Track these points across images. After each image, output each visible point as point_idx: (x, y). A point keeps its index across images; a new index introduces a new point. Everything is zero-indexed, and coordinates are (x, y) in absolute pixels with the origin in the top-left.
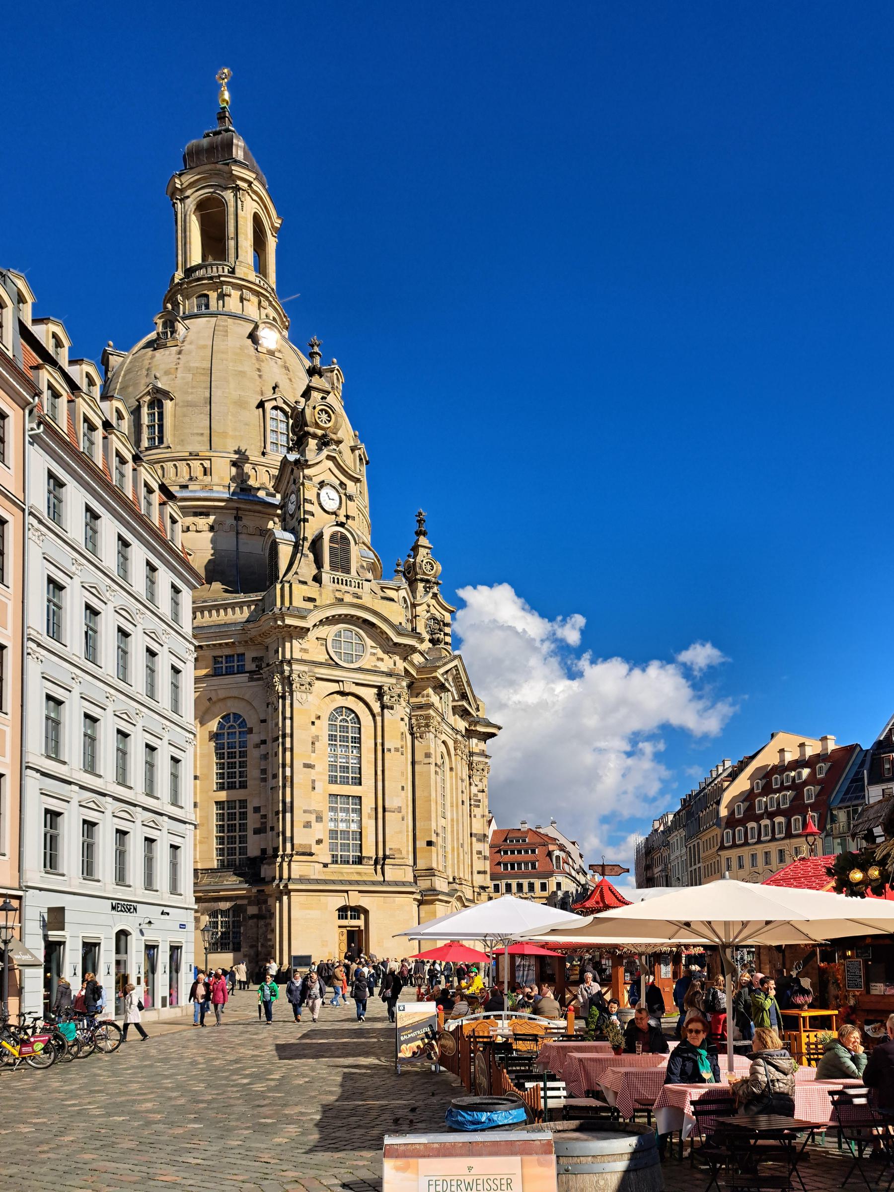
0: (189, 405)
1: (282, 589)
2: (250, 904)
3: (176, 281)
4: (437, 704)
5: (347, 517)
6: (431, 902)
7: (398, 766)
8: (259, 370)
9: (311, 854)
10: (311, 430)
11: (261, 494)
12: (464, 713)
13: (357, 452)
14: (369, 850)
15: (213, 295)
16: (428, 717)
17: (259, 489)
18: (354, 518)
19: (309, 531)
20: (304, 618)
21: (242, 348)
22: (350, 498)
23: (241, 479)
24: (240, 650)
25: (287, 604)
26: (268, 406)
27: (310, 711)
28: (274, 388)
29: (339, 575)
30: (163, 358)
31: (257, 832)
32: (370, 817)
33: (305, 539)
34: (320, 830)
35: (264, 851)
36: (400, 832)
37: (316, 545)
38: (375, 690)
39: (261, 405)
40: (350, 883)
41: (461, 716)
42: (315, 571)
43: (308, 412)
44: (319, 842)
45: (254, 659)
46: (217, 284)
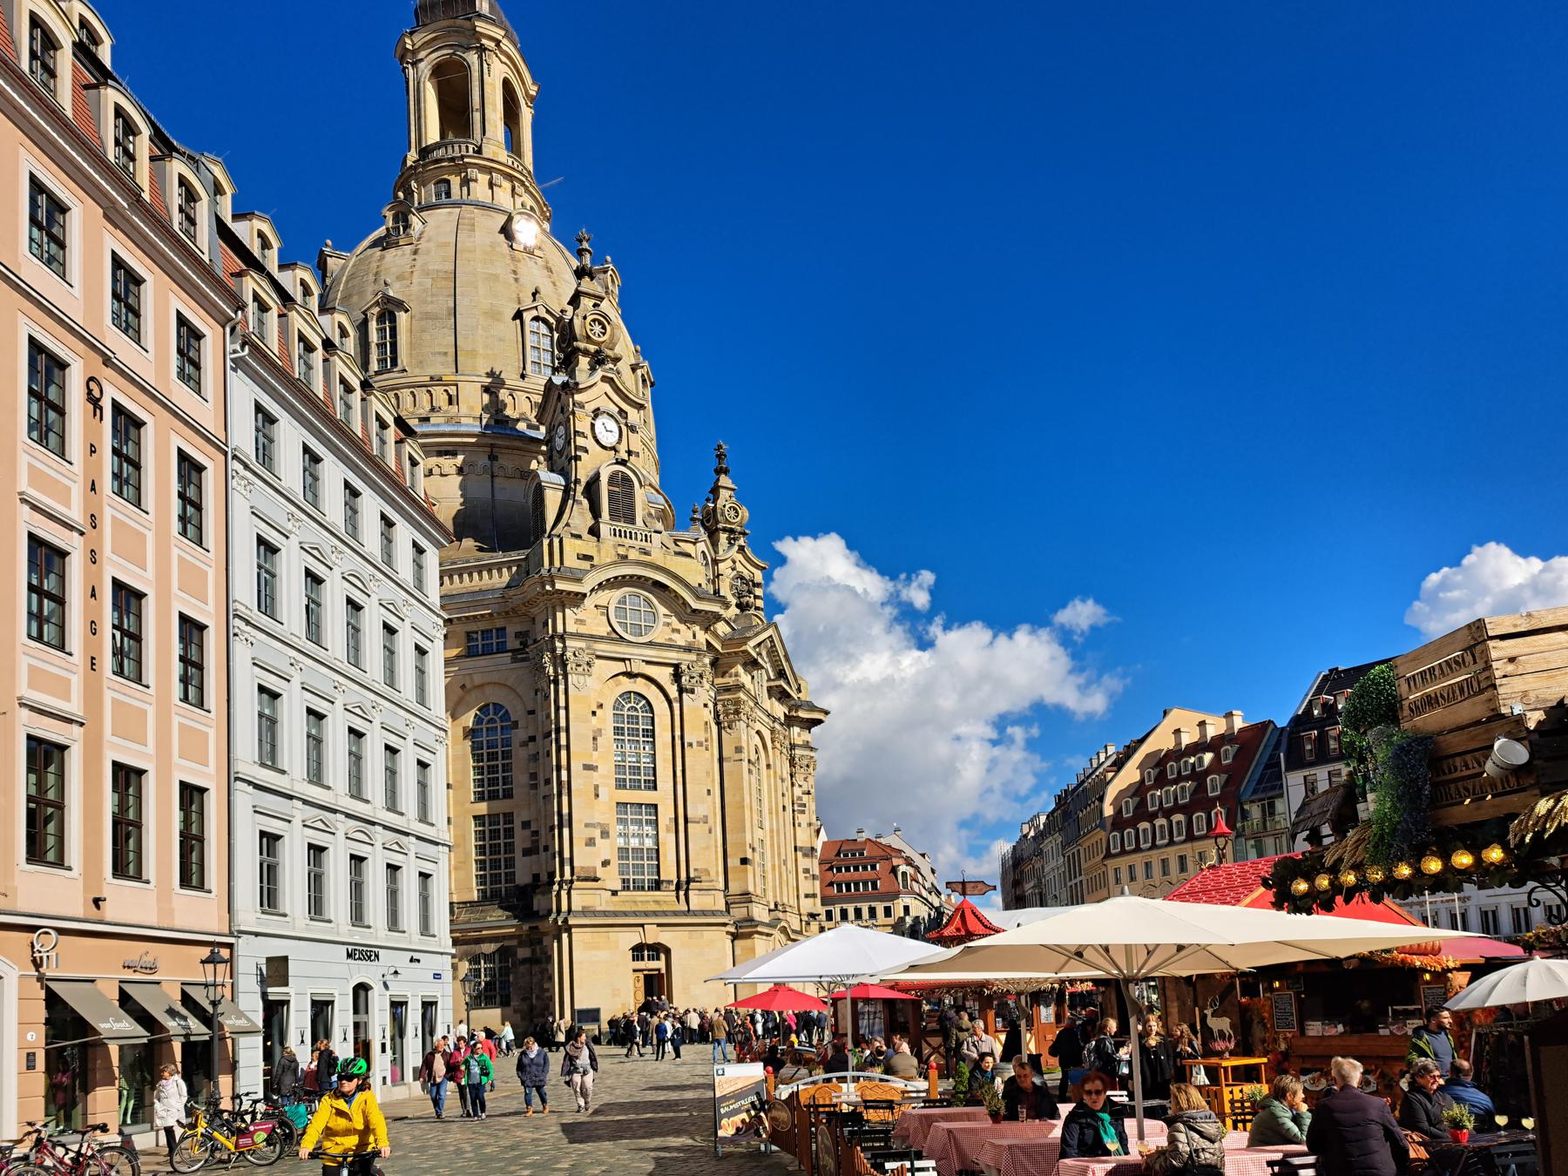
0: (427, 316)
1: (551, 545)
2: (521, 944)
3: (409, 163)
4: (748, 685)
5: (629, 453)
7: (701, 764)
8: (515, 272)
9: (596, 880)
10: (582, 345)
11: (521, 426)
12: (783, 696)
13: (639, 372)
14: (669, 872)
15: (455, 181)
16: (737, 702)
17: (518, 420)
18: (637, 455)
19: (583, 472)
20: (579, 580)
21: (493, 246)
22: (632, 429)
23: (495, 408)
24: (499, 623)
25: (557, 563)
26: (527, 316)
27: (590, 699)
28: (534, 295)
30: (395, 259)
31: (526, 853)
32: (668, 831)
33: (577, 481)
34: (606, 849)
35: (536, 877)
36: (708, 848)
37: (592, 489)
38: (671, 670)
39: (518, 315)
40: (646, 914)
41: (779, 700)
42: (591, 522)
43: (577, 322)
44: (606, 863)
45: (517, 635)
46: (459, 166)
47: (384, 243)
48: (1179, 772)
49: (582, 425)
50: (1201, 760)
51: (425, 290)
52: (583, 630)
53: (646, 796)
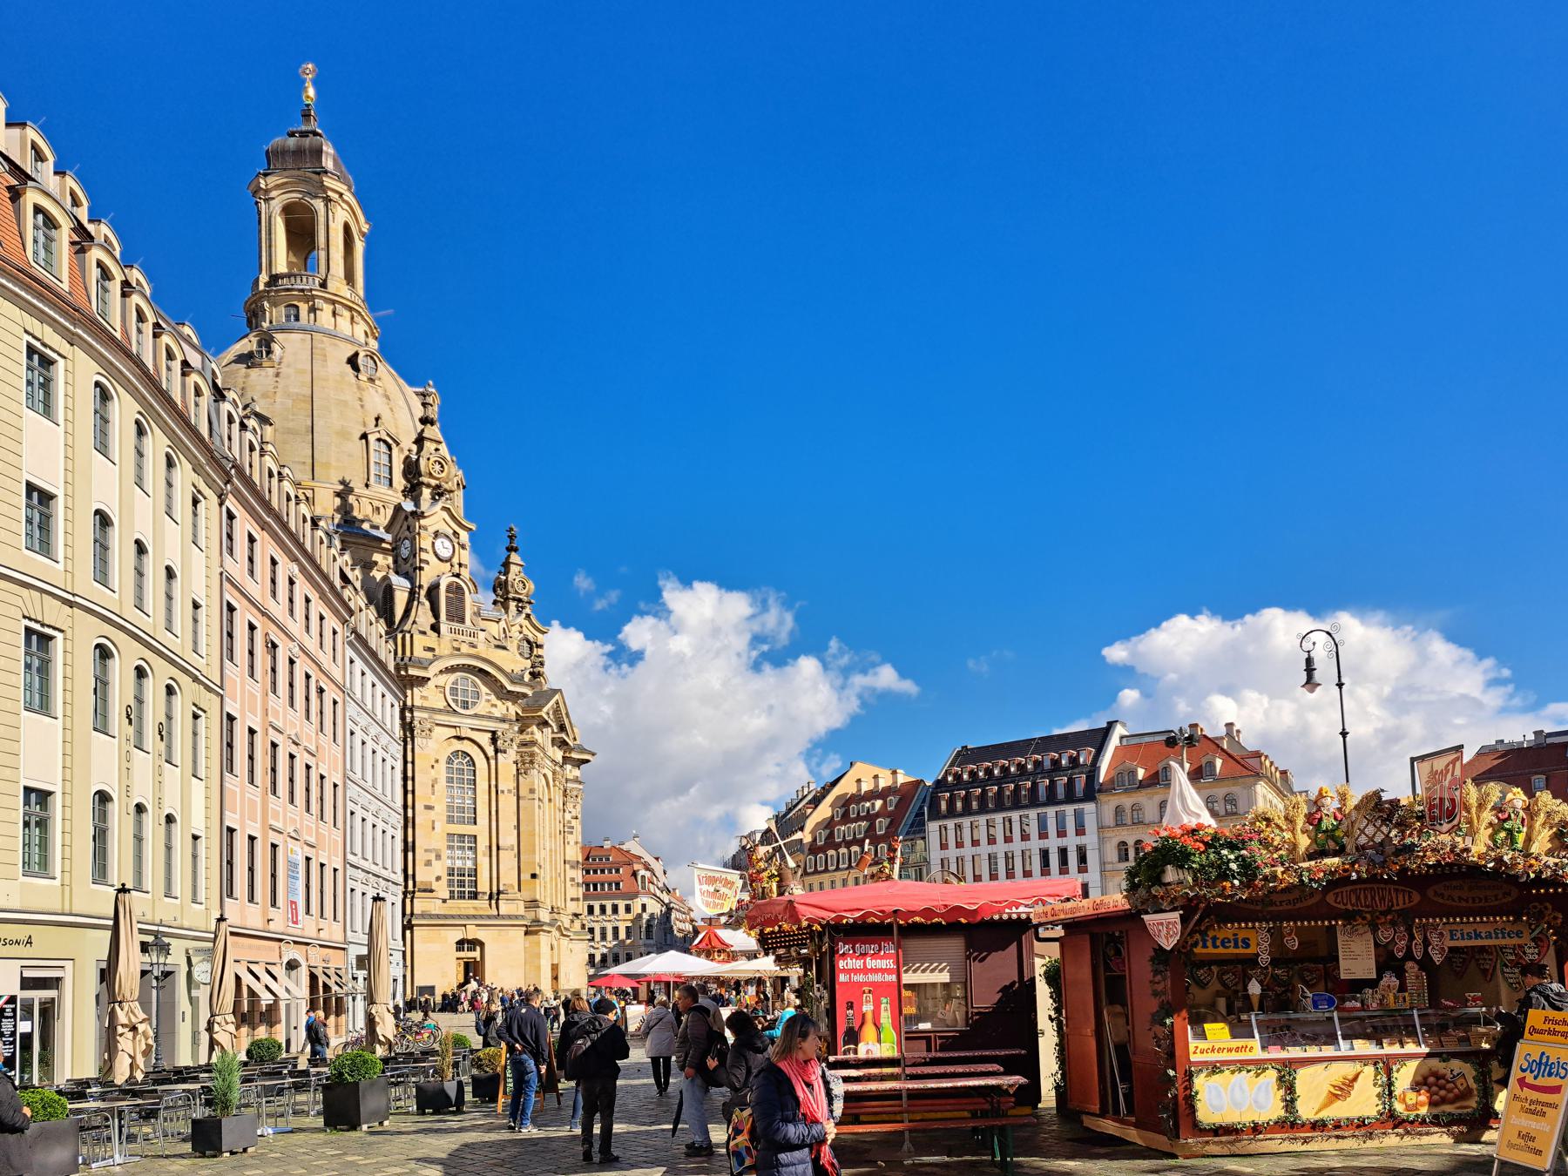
0: (290, 431)
1: (403, 638)
3: (261, 287)
7: (507, 803)
9: (432, 891)
10: (425, 479)
11: (366, 526)
12: (563, 744)
14: (483, 886)
15: (304, 308)
16: (532, 755)
21: (343, 375)
26: (372, 438)
28: (377, 419)
29: (456, 625)
30: (258, 378)
34: (440, 868)
39: (364, 436)
40: (468, 917)
43: (423, 462)
44: (438, 879)
47: (247, 359)
52: (426, 704)
53: (468, 829)
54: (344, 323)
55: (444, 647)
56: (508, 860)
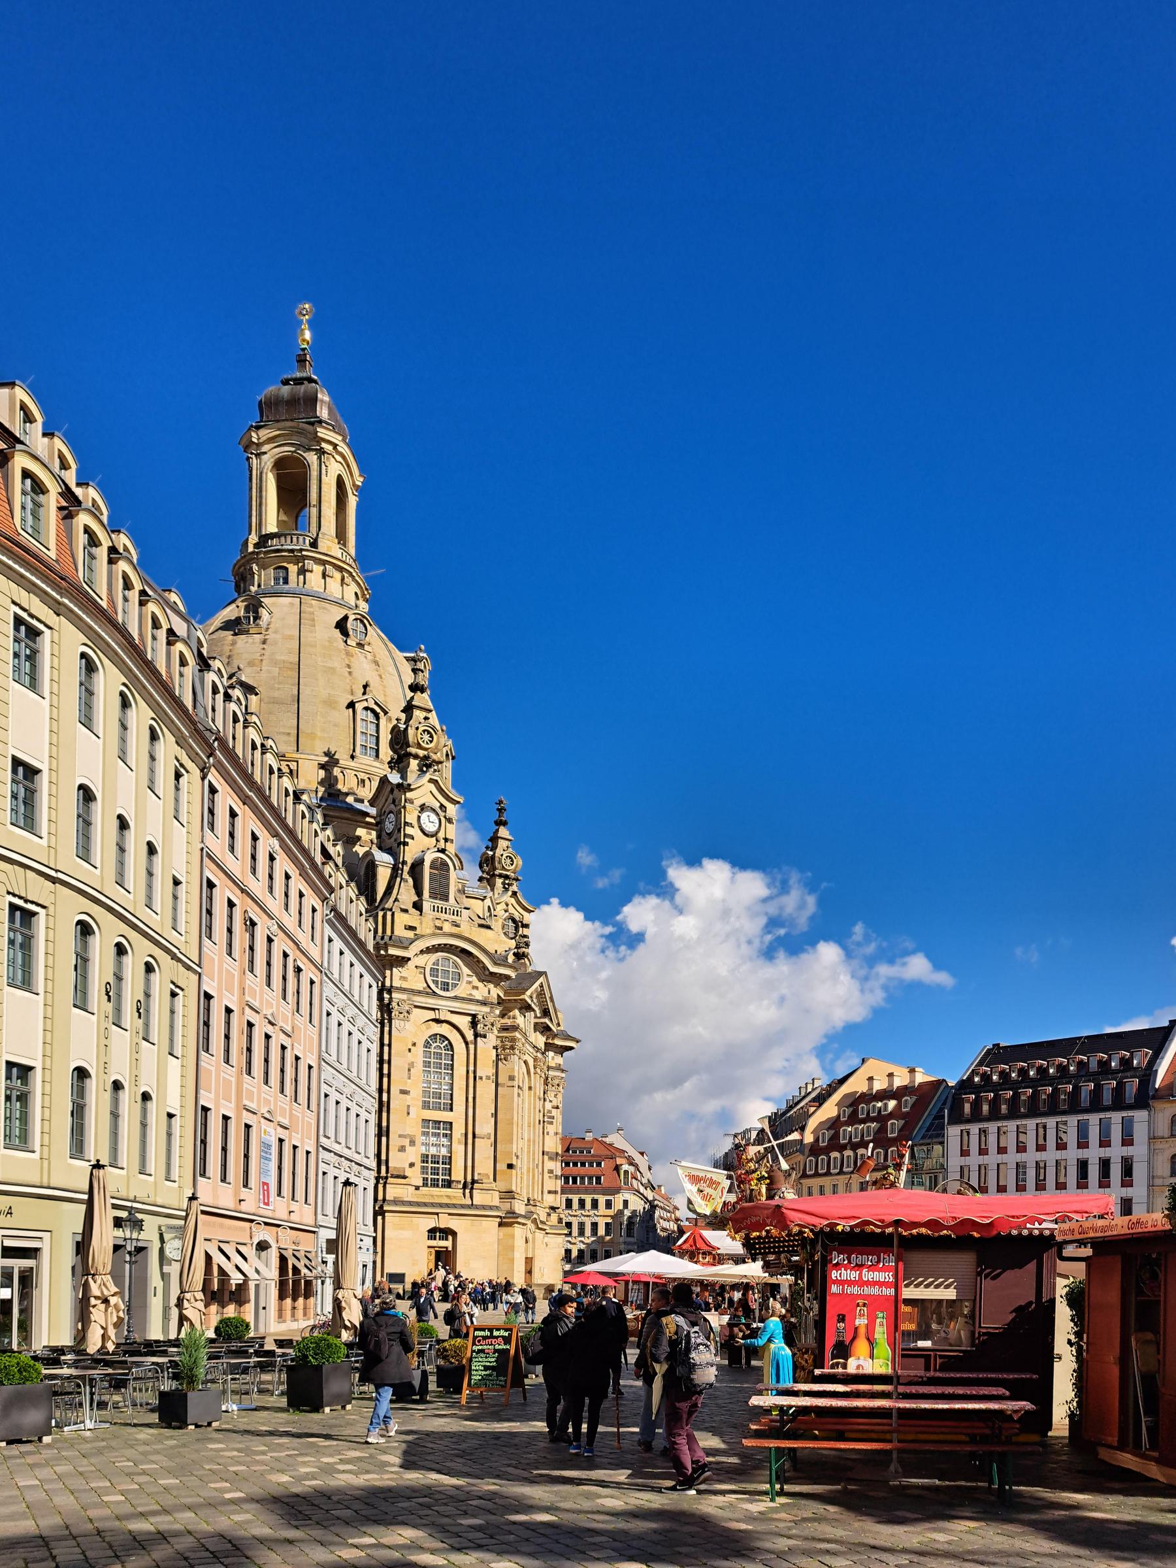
3: (251, 549)
4: (522, 1026)
6: (510, 1225)
7: (485, 1090)
8: (349, 666)
12: (545, 1029)
14: (458, 1175)
15: (293, 569)
16: (513, 1040)
17: (347, 794)
18: (452, 841)
19: (409, 855)
20: (406, 948)
21: (331, 640)
22: (450, 821)
23: (329, 782)
25: (389, 932)
28: (365, 687)
30: (246, 645)
32: (459, 1142)
33: (404, 863)
37: (416, 868)
38: (469, 1019)
39: (351, 705)
40: (441, 1205)
41: (542, 1033)
44: (412, 1165)
46: (298, 558)
47: (233, 626)
48: (868, 1113)
49: (411, 817)
50: (886, 1105)
51: (274, 678)
54: (334, 586)
55: (426, 924)
56: (484, 1149)
